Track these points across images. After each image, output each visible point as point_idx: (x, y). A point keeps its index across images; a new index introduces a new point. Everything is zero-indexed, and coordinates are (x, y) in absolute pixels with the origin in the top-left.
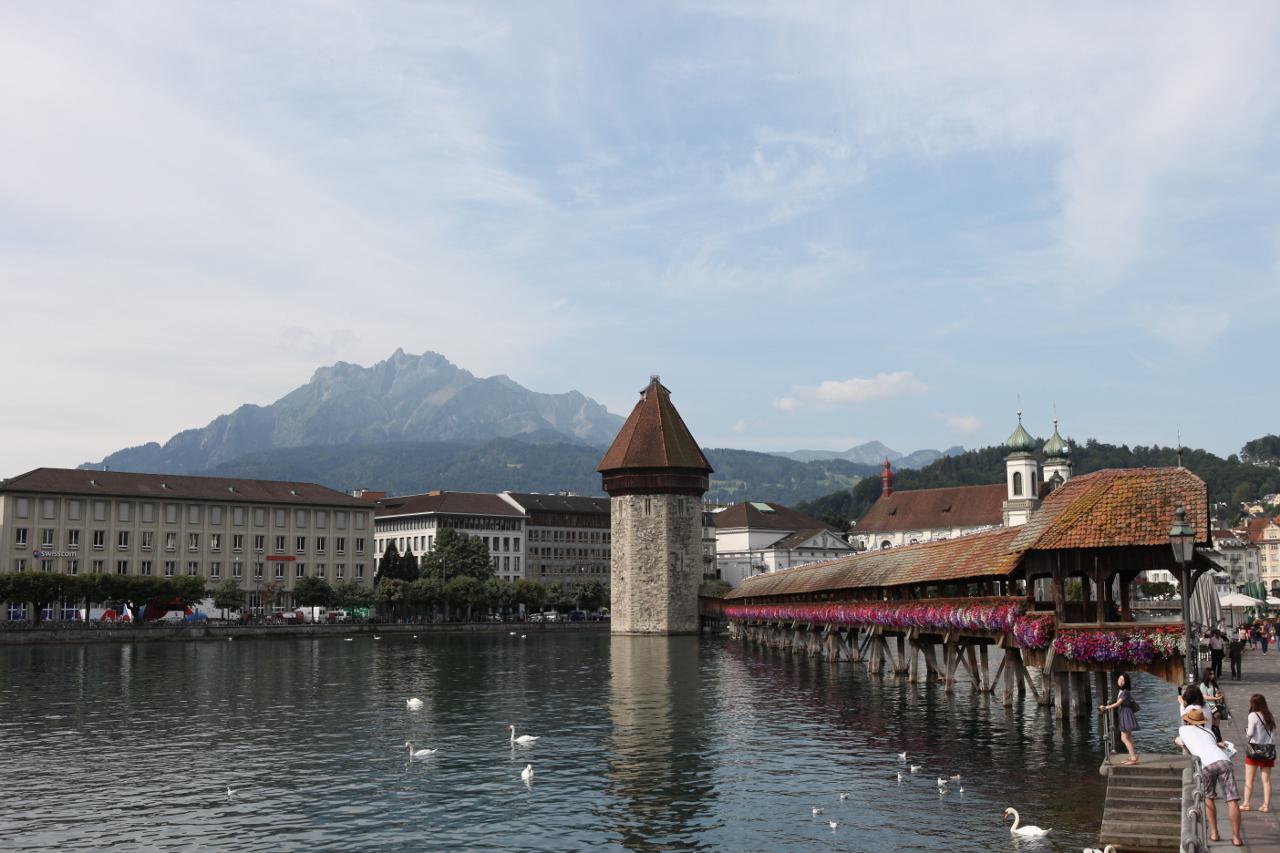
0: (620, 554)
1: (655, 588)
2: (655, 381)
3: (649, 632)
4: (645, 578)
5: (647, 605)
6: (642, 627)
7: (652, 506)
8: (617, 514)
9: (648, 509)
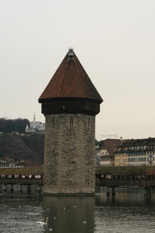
0: (70, 147)
1: (91, 168)
2: (71, 51)
3: (88, 193)
4: (87, 163)
5: (87, 178)
6: (86, 190)
7: (90, 121)
8: (68, 124)
9: (89, 124)
